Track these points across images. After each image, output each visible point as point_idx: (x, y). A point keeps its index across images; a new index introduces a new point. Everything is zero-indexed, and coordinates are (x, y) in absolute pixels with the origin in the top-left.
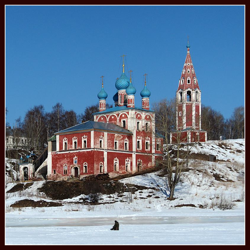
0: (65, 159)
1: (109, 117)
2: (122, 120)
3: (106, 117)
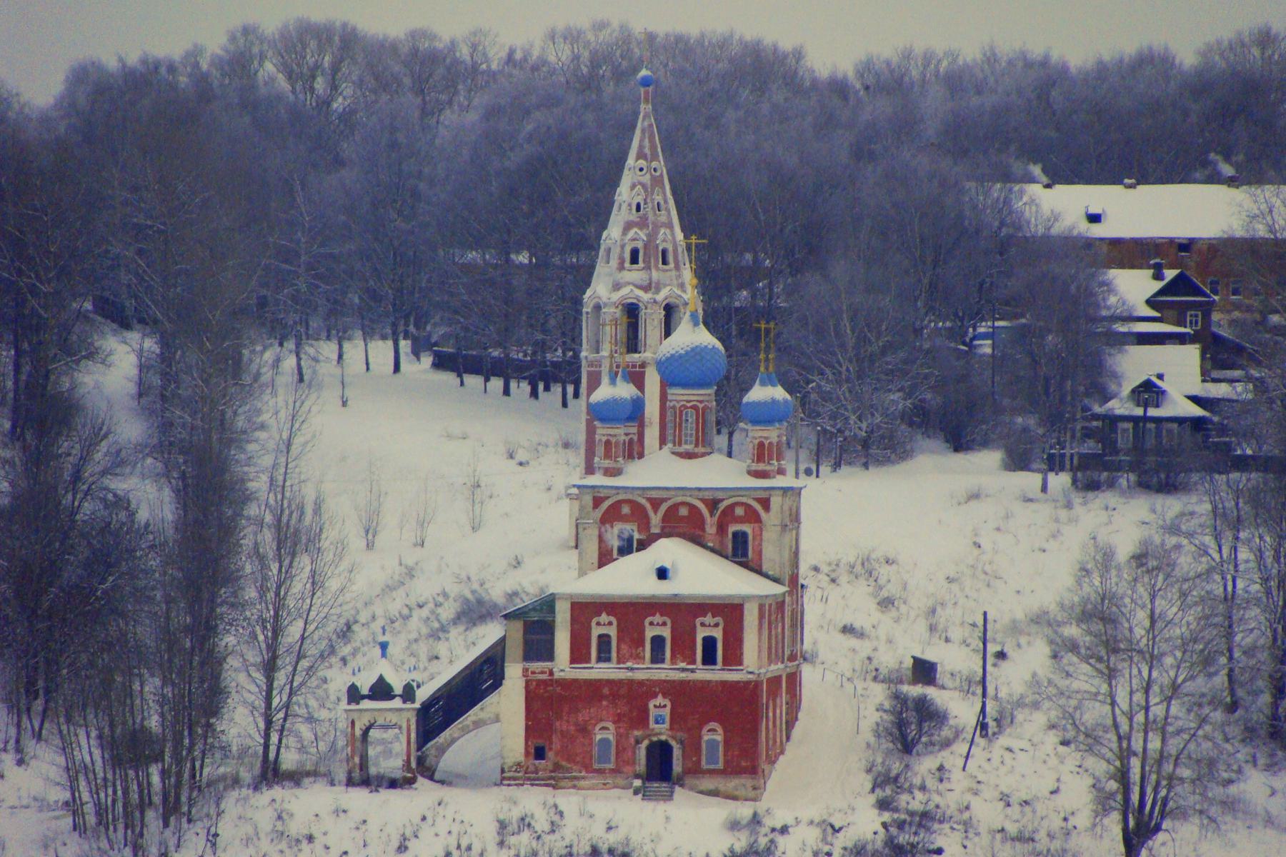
0: (600, 701)
1: (664, 507)
2: (733, 528)
3: (648, 506)
